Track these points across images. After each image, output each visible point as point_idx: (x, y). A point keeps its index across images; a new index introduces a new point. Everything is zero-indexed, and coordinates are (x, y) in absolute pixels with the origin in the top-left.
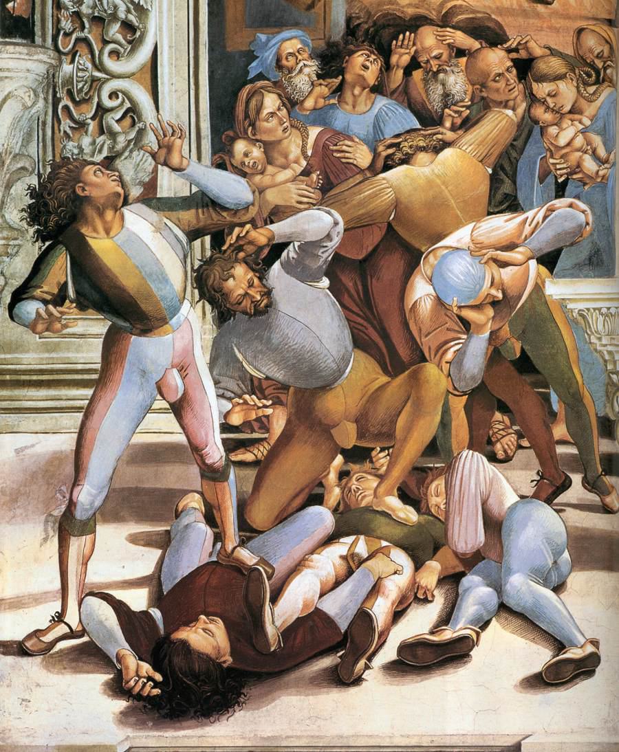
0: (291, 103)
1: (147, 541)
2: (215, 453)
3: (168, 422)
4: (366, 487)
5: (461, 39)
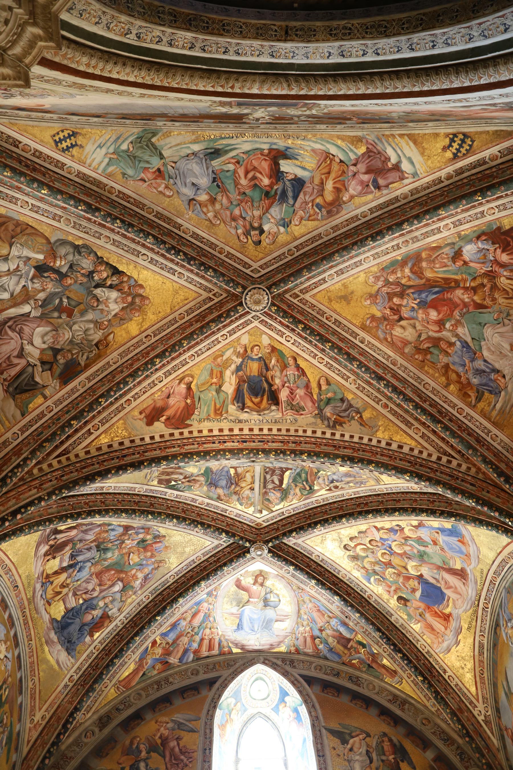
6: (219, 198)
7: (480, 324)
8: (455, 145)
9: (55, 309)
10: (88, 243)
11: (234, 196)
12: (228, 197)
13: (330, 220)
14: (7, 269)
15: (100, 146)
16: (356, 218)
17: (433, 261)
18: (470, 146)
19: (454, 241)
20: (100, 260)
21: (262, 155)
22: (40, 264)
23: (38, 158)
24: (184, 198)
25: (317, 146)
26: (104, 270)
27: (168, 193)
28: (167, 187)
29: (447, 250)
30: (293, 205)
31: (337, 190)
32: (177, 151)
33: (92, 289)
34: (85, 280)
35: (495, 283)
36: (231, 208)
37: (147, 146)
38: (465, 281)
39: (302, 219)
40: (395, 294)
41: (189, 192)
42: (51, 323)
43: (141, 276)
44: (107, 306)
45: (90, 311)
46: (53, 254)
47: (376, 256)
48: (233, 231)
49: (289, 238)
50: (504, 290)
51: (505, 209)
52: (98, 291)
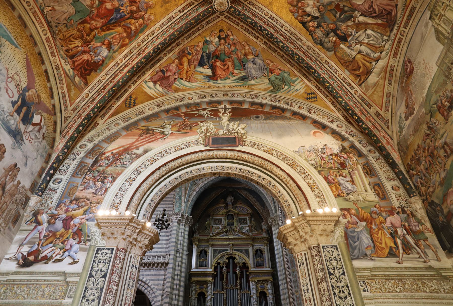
0: (65, 205)
1: (29, 247)
2: (42, 238)
3: (38, 234)
4: (58, 242)
5: (86, 200)
6: (242, 56)
7: (79, 12)
8: (132, 101)
9: (345, 12)
10: (315, 45)
11: (234, 56)
12: (237, 56)
13: (183, 48)
14: (362, 46)
15: (297, 90)
16: (169, 52)
17: (121, 38)
18: (126, 104)
19: (114, 54)
20: (311, 33)
21: (221, 77)
22: (344, 42)
23: (326, 94)
24: (260, 58)
25: (194, 84)
26: (310, 26)
27: (268, 61)
28: (269, 64)
29: (116, 48)
30: (203, 52)
31: (181, 64)
32: (262, 81)
33: (320, 17)
34: (323, 24)
35: (82, 40)
36: (236, 50)
37: (276, 86)
38: (99, 33)
39: (198, 46)
40: (136, 12)
41: (258, 61)
42: (351, 4)
43: (290, 18)
44: (314, 3)
45: (325, 4)
46: (335, 47)
47: (153, 32)
48: (235, 37)
49: (204, 34)
50: (76, 39)
51: (98, 82)
52: (317, 14)
